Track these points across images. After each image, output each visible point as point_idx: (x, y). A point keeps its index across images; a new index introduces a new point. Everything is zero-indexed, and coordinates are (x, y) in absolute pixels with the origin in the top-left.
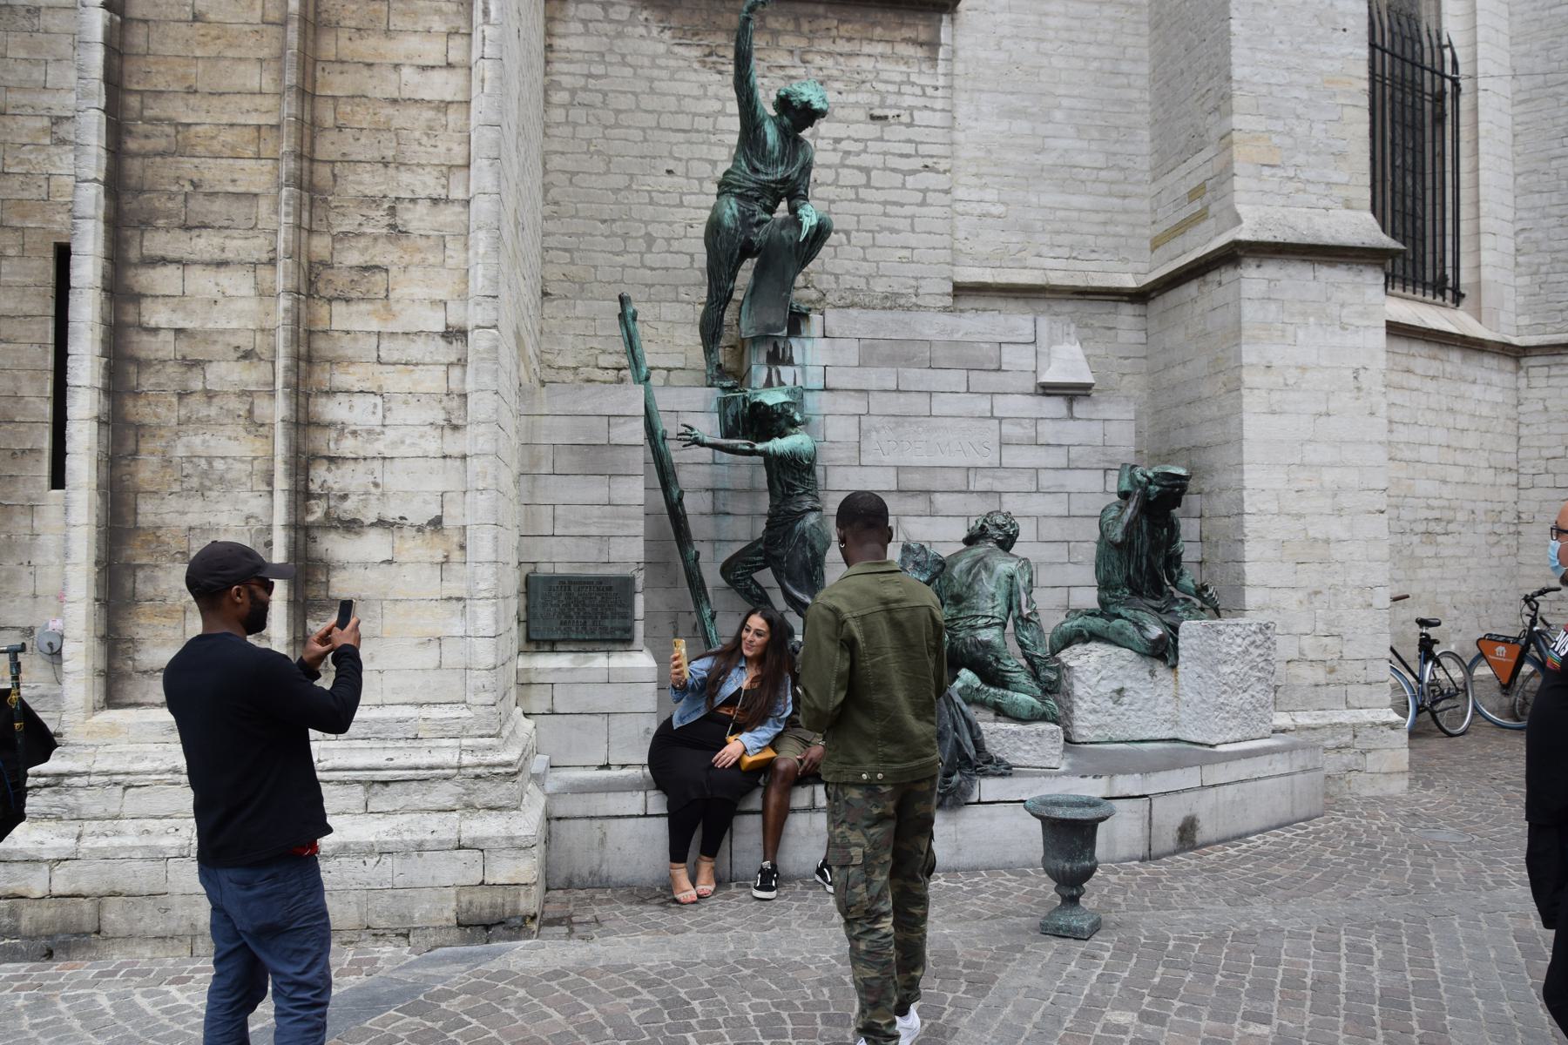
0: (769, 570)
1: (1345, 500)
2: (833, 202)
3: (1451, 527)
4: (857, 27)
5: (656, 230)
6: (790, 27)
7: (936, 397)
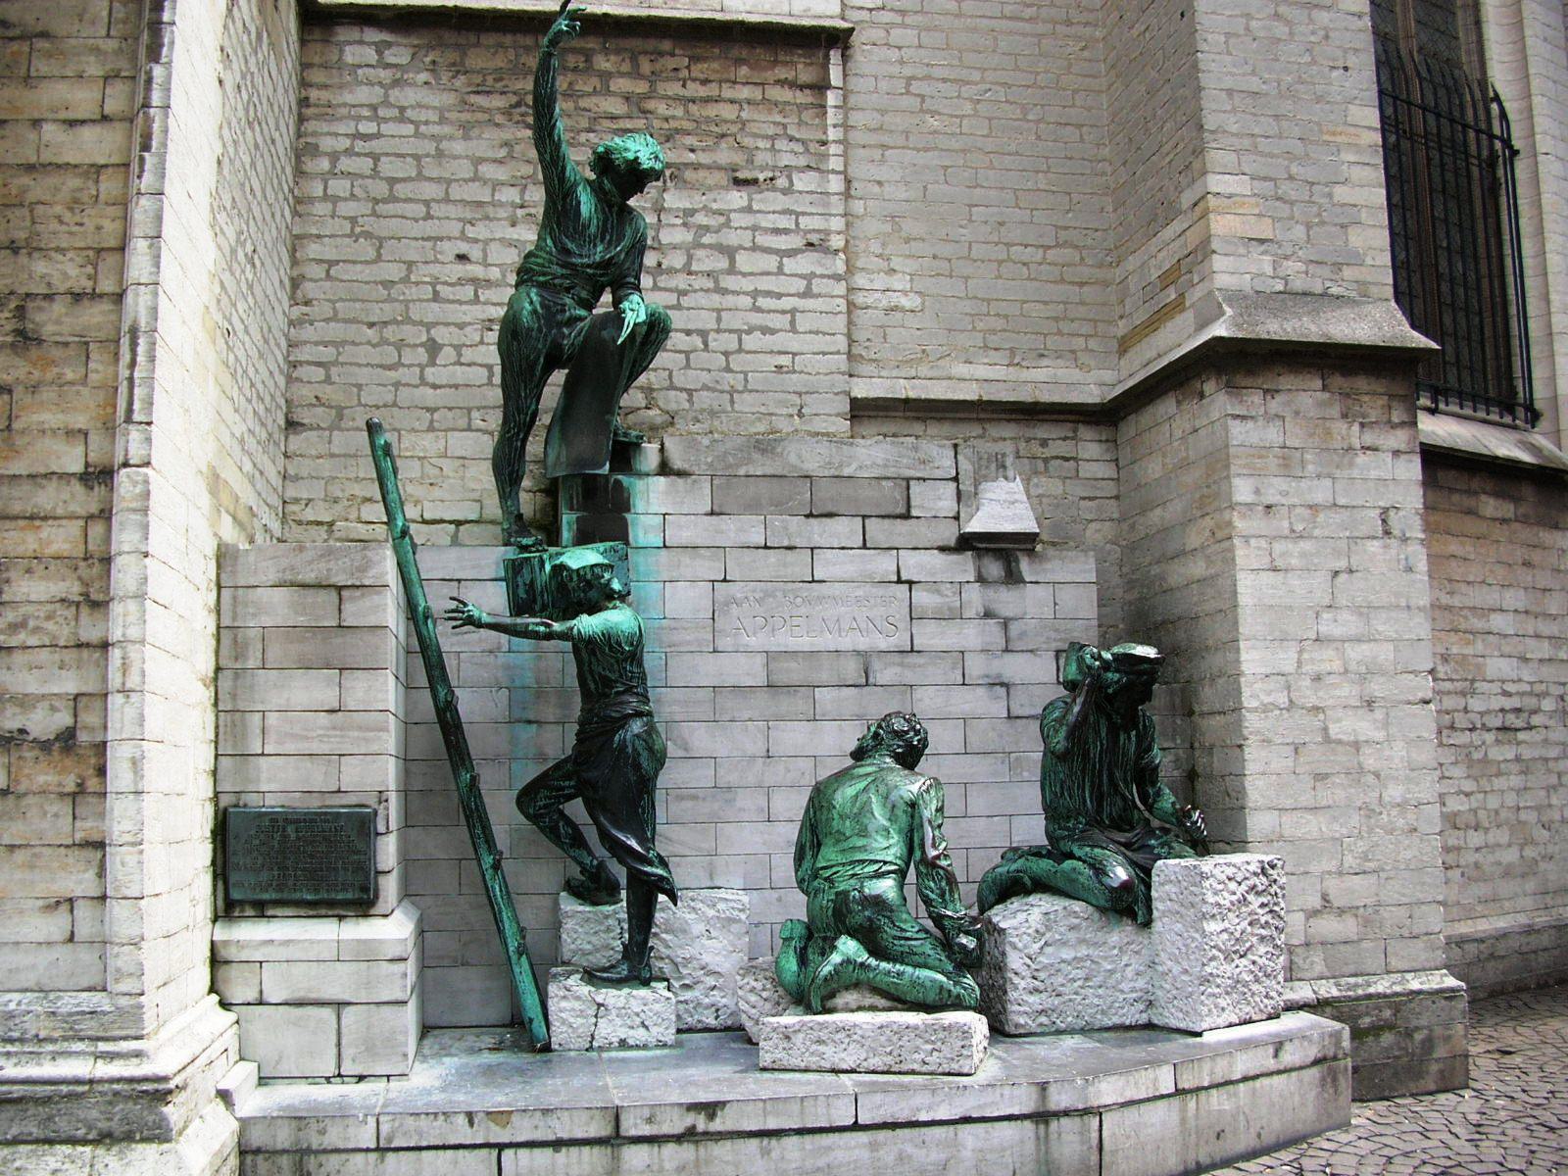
0: (579, 802)
1: (1377, 688)
2: (683, 293)
3: (1536, 720)
4: (715, 65)
5: (441, 335)
6: (626, 67)
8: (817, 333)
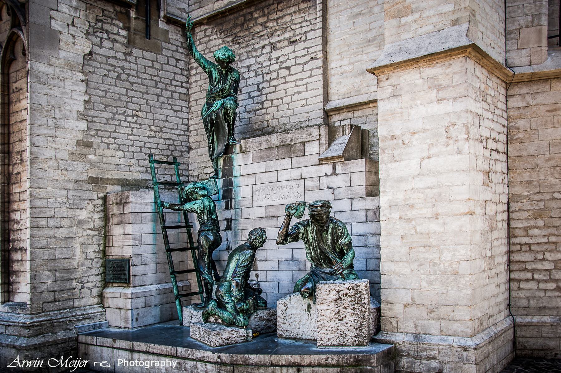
2: (276, 86)
7: (279, 173)
8: (313, 90)
